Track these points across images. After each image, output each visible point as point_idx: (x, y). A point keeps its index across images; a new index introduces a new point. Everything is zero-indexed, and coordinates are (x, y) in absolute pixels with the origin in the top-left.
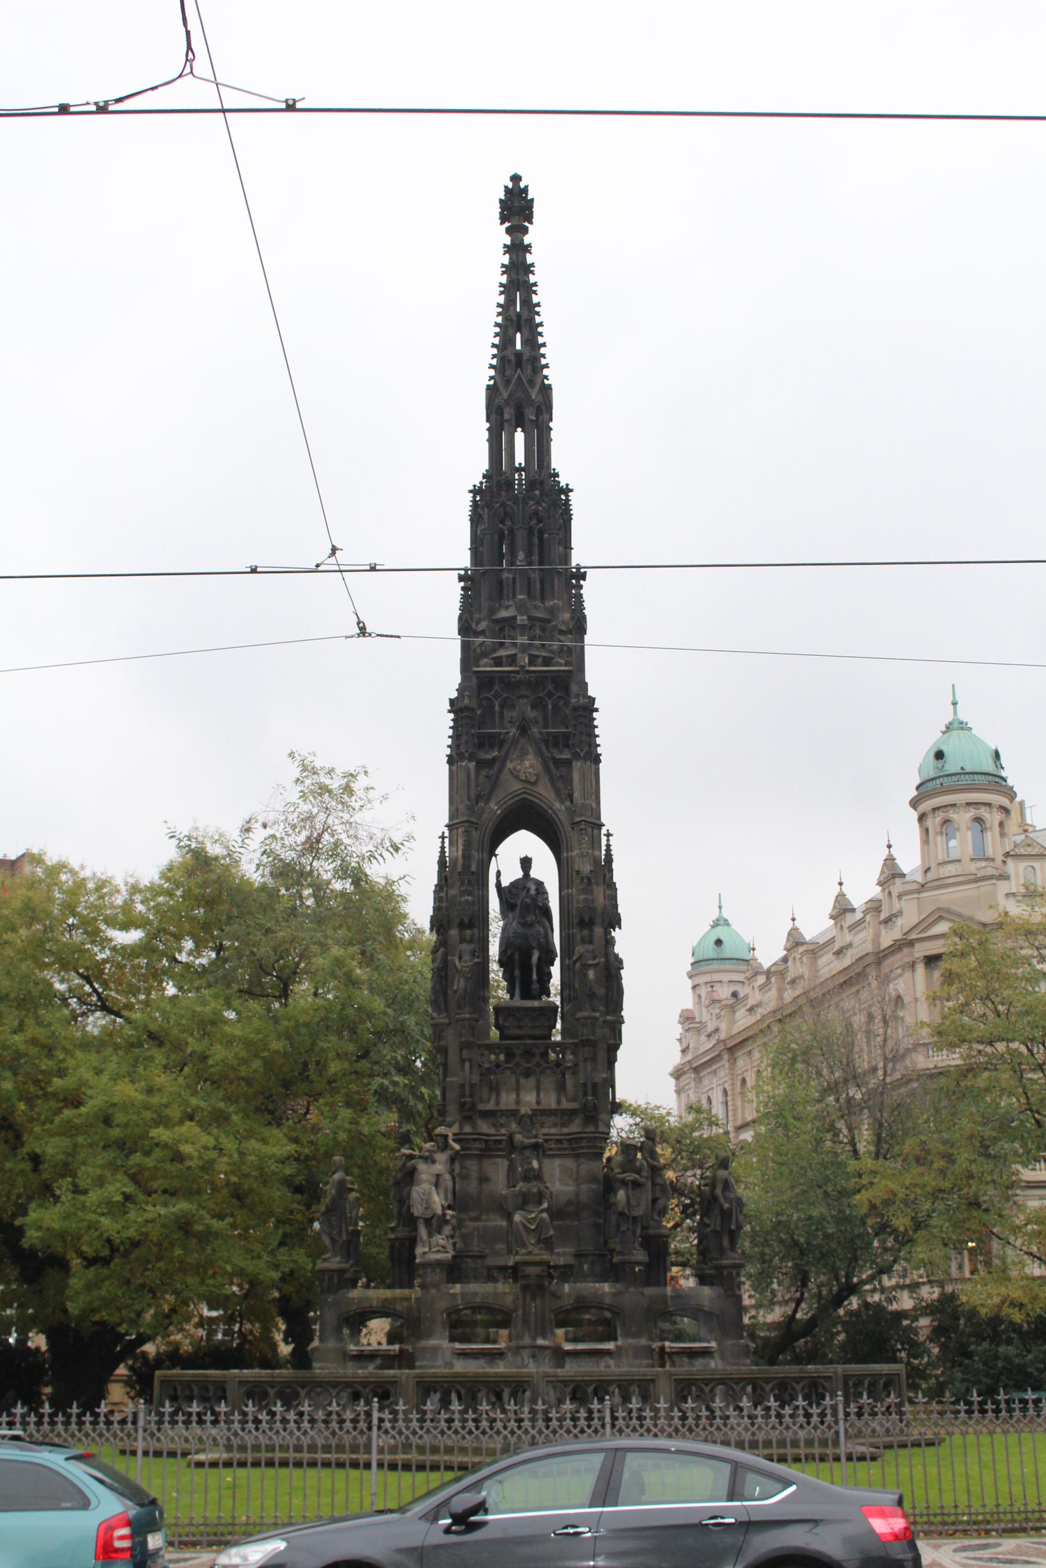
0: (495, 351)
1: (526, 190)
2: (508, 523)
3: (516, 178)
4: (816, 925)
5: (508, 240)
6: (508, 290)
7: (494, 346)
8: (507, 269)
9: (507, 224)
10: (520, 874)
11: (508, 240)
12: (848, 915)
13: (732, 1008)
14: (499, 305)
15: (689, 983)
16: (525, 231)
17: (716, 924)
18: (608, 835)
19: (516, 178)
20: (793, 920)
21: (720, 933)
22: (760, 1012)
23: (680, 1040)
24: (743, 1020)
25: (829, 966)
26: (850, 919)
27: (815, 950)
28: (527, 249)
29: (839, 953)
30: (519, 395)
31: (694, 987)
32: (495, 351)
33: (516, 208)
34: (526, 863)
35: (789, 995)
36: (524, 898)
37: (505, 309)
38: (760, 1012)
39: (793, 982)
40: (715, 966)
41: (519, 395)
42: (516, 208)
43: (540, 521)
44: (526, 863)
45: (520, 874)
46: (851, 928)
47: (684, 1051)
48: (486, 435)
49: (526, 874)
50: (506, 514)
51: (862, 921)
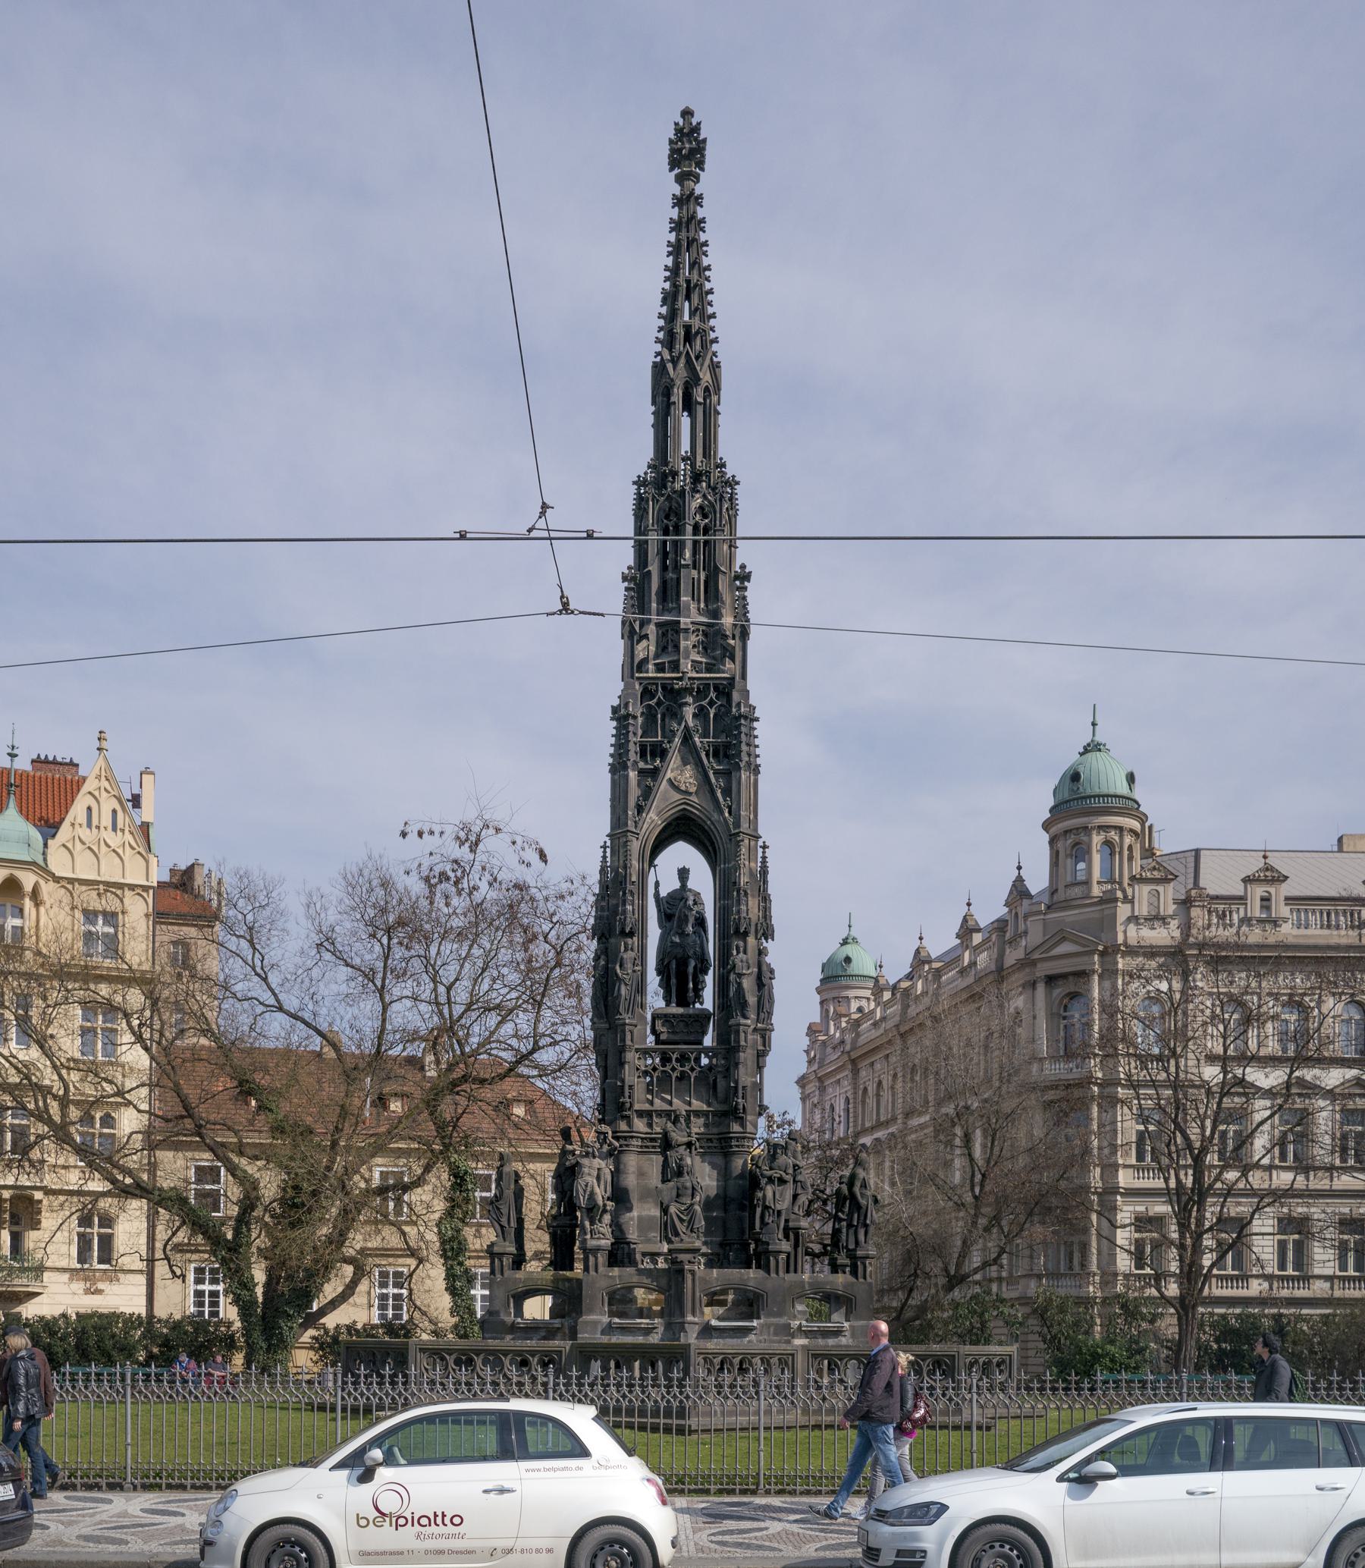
0: (662, 322)
1: (696, 129)
3: (687, 113)
5: (677, 190)
6: (676, 250)
7: (660, 316)
8: (677, 226)
9: (677, 171)
10: (677, 885)
11: (677, 190)
14: (667, 269)
16: (697, 179)
19: (687, 113)
30: (685, 377)
32: (662, 322)
33: (687, 151)
34: (683, 874)
36: (676, 910)
37: (674, 271)
41: (685, 377)
42: (687, 151)
43: (705, 516)
44: (683, 874)
45: (677, 885)
48: (651, 419)
49: (684, 885)
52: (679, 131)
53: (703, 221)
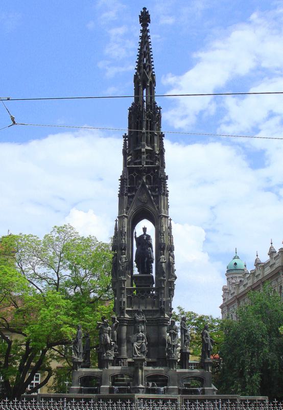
1: (148, 12)
2: (140, 119)
3: (145, 9)
4: (265, 258)
5: (142, 28)
6: (141, 44)
8: (142, 38)
10: (143, 233)
11: (142, 28)
12: (274, 254)
13: (239, 286)
15: (226, 278)
16: (148, 25)
17: (235, 258)
18: (170, 220)
19: (145, 9)
20: (257, 256)
21: (236, 261)
22: (248, 286)
23: (223, 296)
24: (242, 289)
25: (268, 271)
26: (275, 255)
27: (264, 266)
28: (148, 31)
29: (271, 266)
31: (227, 279)
33: (145, 18)
34: (145, 229)
35: (256, 280)
36: (144, 241)
37: (141, 50)
38: (248, 286)
39: (257, 276)
40: (234, 271)
42: (145, 18)
44: (145, 229)
45: (143, 233)
46: (275, 258)
47: (224, 300)
49: (145, 234)
50: (139, 116)
51: (278, 255)
52: (142, 13)
53: (150, 36)
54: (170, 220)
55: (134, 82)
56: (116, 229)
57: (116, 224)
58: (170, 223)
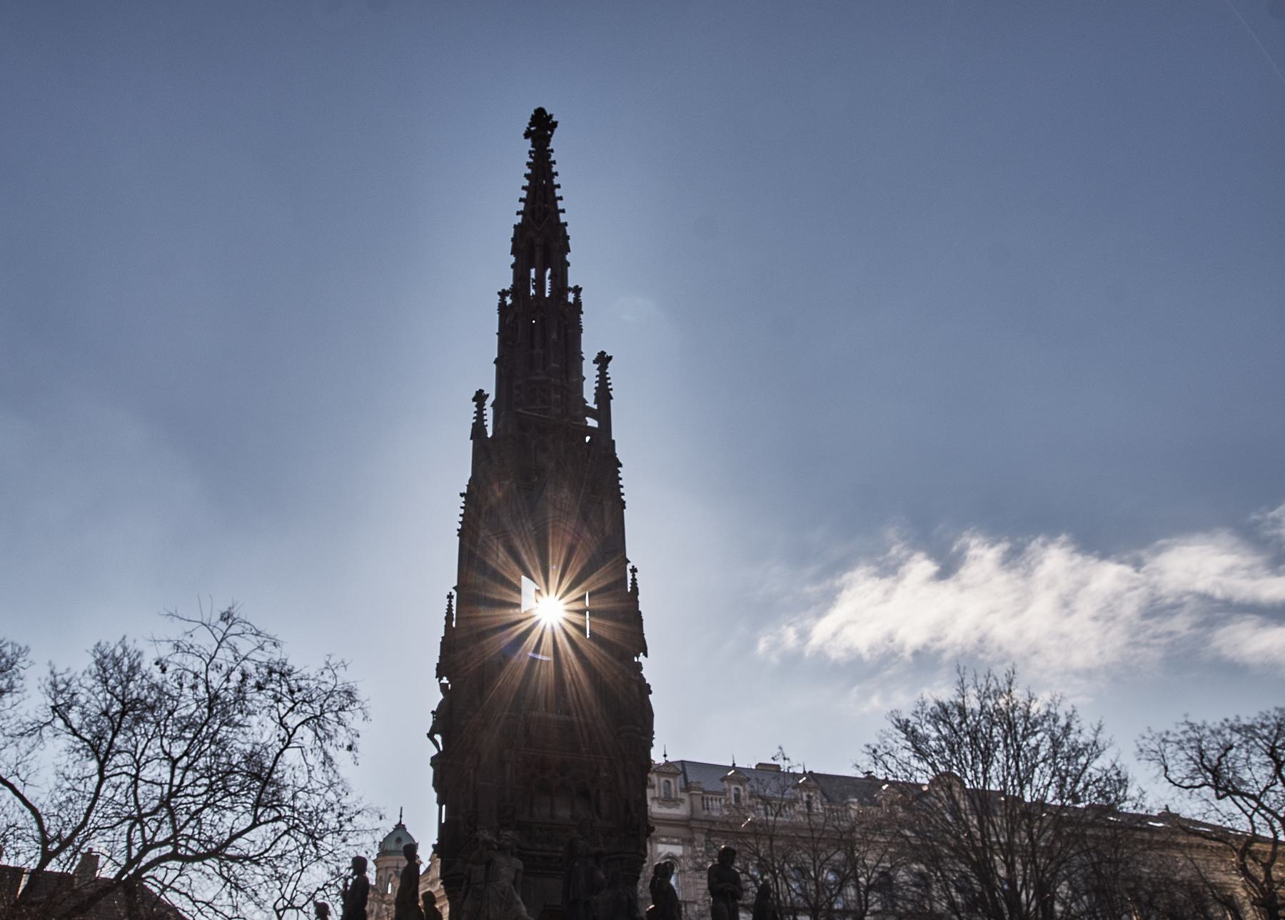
33: (541, 127)
42: (541, 127)
54: (634, 570)
55: (514, 251)
56: (449, 618)
57: (450, 606)
58: (634, 580)
